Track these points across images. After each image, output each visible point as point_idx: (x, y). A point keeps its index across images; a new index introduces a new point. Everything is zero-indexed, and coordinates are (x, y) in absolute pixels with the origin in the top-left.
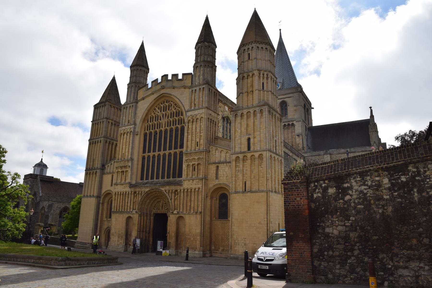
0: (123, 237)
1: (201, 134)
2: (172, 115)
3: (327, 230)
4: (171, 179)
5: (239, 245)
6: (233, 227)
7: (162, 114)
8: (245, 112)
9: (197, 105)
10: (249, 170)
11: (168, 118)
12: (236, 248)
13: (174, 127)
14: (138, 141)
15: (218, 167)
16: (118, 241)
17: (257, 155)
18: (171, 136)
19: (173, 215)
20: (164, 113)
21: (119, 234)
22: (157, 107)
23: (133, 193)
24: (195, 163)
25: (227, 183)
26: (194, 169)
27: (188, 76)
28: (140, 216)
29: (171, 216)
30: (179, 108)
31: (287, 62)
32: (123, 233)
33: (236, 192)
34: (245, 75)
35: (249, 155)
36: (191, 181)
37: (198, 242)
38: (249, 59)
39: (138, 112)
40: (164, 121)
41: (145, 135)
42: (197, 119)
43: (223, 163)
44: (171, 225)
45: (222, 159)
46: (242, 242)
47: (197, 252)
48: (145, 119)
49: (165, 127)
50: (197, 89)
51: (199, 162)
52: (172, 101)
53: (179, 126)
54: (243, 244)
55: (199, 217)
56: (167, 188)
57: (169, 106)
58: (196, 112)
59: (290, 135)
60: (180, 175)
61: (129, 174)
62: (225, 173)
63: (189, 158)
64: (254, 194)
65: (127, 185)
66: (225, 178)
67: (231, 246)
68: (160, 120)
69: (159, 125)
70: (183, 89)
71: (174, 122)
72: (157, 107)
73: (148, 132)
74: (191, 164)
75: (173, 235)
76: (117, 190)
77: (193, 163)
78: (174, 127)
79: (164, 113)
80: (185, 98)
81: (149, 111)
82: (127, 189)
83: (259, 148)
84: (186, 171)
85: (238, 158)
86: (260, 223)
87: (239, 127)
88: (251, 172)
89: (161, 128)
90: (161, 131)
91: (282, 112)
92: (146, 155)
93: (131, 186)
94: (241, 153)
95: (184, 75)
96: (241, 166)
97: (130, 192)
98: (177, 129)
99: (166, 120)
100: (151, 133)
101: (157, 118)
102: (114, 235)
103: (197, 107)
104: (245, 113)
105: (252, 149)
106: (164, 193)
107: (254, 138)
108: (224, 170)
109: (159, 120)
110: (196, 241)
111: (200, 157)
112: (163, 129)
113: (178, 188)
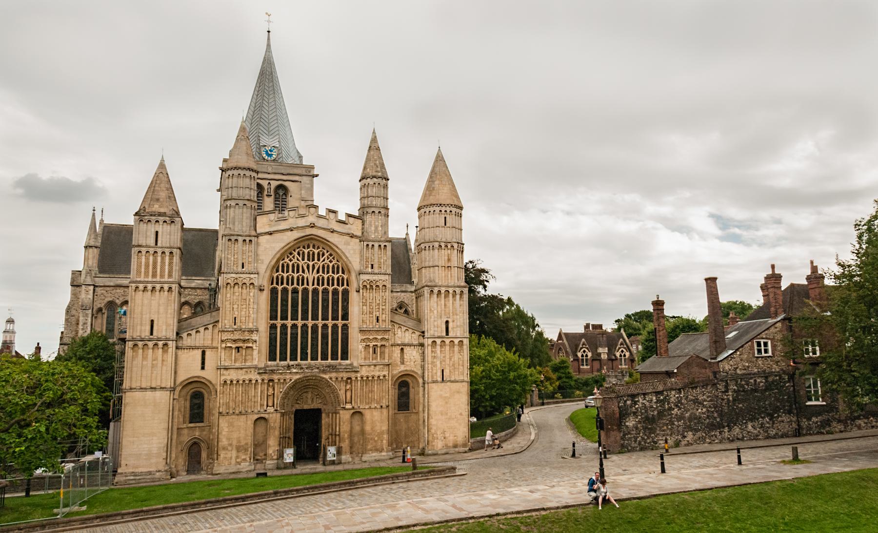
0: (249, 449)
1: (384, 307)
4: (329, 360)
5: (437, 439)
6: (431, 420)
7: (306, 265)
8: (443, 290)
9: (376, 266)
10: (448, 357)
11: (318, 272)
12: (434, 443)
13: (331, 289)
15: (402, 349)
16: (237, 457)
17: (456, 341)
18: (325, 300)
19: (345, 411)
20: (311, 263)
21: (240, 446)
22: (294, 250)
23: (266, 381)
24: (376, 344)
25: (415, 370)
26: (374, 352)
27: (356, 219)
28: (283, 415)
29: (341, 412)
30: (338, 261)
31: (269, 96)
32: (249, 444)
33: (434, 382)
34: (443, 245)
35: (447, 341)
36: (373, 366)
37: (385, 442)
38: (445, 225)
39: (260, 252)
40: (310, 276)
41: (274, 292)
42: (377, 286)
43: (410, 345)
44: (342, 424)
45: (406, 341)
46: (441, 435)
47: (383, 454)
49: (313, 285)
50: (376, 245)
51: (383, 343)
52: (323, 248)
53: (340, 289)
54: (443, 438)
55: (385, 411)
56: (334, 375)
57: (319, 254)
58: (376, 277)
60: (345, 356)
61: (255, 353)
62: (412, 358)
63: (367, 337)
64: (455, 384)
65: (252, 370)
66: (412, 363)
67: (428, 441)
68: (303, 271)
70: (347, 238)
71: (331, 282)
72: (294, 250)
73: (280, 288)
74: (371, 345)
75: (346, 435)
76: (229, 378)
77: (374, 344)
78: (331, 289)
79: (311, 263)
80: (352, 252)
81: (282, 255)
82: (254, 376)
83: (459, 335)
84: (363, 353)
85: (434, 342)
86: (461, 414)
87: (436, 306)
88: (450, 359)
89: (305, 286)
90: (305, 291)
91: (275, 204)
92: (279, 322)
93: (263, 371)
94: (439, 337)
95: (349, 216)
96: (439, 352)
97: (260, 381)
98: (335, 292)
99: (316, 276)
100: (285, 290)
102: (227, 449)
103: (376, 270)
104: (443, 292)
105: (451, 334)
106: (329, 382)
107: (453, 321)
109: (301, 273)
110: (382, 441)
111: (385, 337)
112: (311, 288)
113: (353, 375)
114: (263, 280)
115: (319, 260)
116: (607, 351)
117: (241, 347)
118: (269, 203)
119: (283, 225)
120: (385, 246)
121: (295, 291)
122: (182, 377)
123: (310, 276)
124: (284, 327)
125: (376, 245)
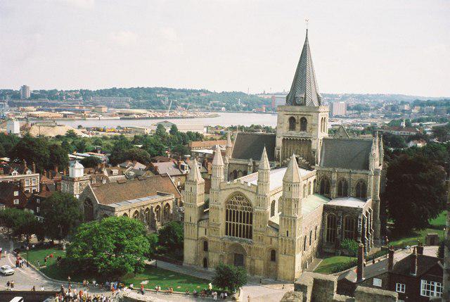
2: (244, 204)
14: (222, 215)
41: (227, 211)
48: (227, 202)
59: (307, 149)
60: (251, 237)
71: (246, 209)
92: (229, 222)
95: (252, 184)
98: (248, 213)
100: (231, 211)
101: (234, 203)
108: (274, 240)
114: (224, 208)
117: (216, 228)
118: (298, 127)
119: (228, 187)
121: (234, 211)
122: (200, 236)
123: (239, 206)
124: (230, 224)
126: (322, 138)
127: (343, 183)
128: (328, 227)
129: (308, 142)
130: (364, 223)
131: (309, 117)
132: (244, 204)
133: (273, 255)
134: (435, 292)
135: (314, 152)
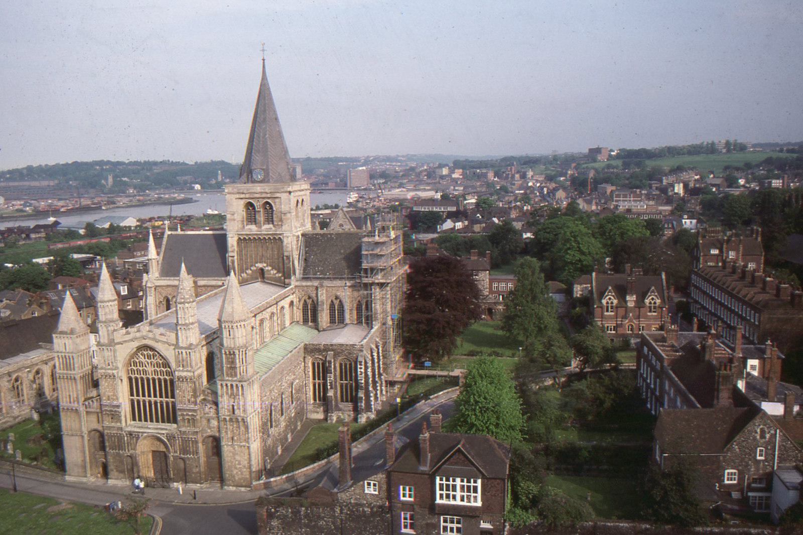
3: (272, 523)
11: (154, 367)
20: (149, 361)
41: (130, 379)
57: (153, 355)
68: (146, 366)
69: (145, 372)
98: (165, 380)
99: (153, 369)
100: (136, 379)
112: (150, 377)
115: (154, 359)
116: (635, 299)
118: (261, 217)
119: (127, 337)
120: (190, 352)
123: (150, 369)
125: (184, 351)
126: (300, 233)
127: (337, 303)
128: (314, 379)
129: (277, 241)
130: (366, 368)
131: (277, 200)
132: (158, 365)
133: (216, 445)
134: (458, 494)
135: (288, 257)
